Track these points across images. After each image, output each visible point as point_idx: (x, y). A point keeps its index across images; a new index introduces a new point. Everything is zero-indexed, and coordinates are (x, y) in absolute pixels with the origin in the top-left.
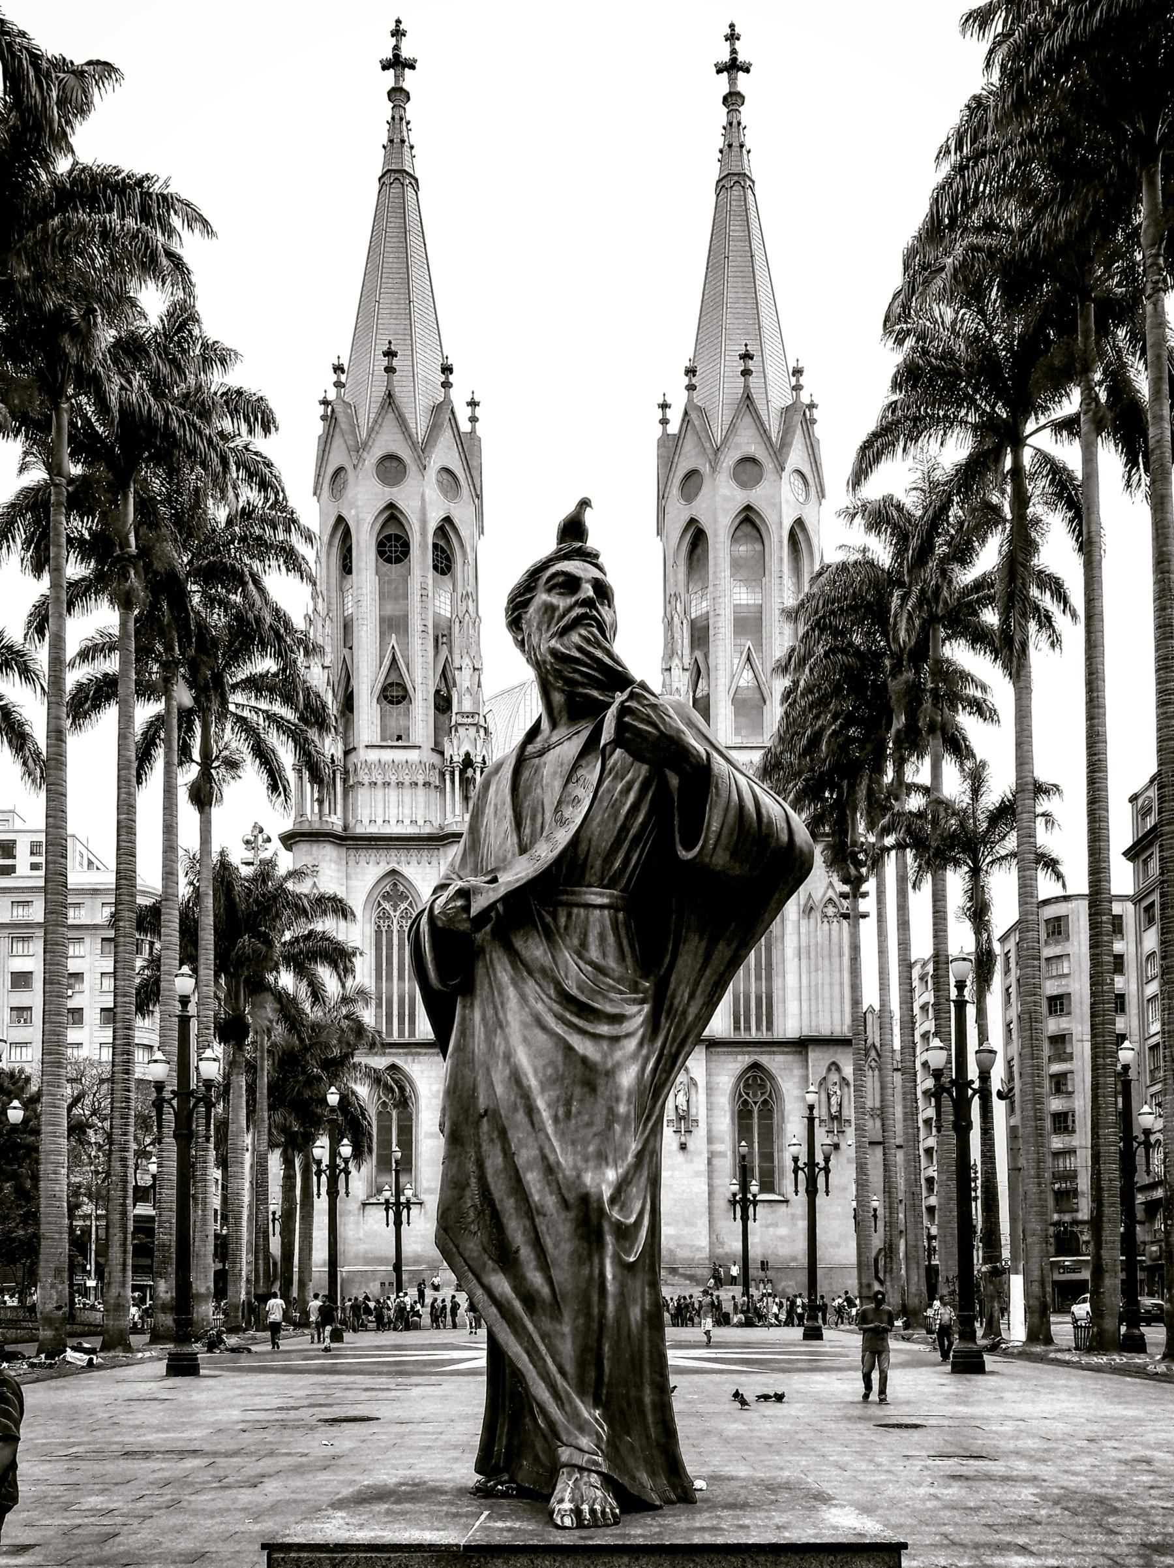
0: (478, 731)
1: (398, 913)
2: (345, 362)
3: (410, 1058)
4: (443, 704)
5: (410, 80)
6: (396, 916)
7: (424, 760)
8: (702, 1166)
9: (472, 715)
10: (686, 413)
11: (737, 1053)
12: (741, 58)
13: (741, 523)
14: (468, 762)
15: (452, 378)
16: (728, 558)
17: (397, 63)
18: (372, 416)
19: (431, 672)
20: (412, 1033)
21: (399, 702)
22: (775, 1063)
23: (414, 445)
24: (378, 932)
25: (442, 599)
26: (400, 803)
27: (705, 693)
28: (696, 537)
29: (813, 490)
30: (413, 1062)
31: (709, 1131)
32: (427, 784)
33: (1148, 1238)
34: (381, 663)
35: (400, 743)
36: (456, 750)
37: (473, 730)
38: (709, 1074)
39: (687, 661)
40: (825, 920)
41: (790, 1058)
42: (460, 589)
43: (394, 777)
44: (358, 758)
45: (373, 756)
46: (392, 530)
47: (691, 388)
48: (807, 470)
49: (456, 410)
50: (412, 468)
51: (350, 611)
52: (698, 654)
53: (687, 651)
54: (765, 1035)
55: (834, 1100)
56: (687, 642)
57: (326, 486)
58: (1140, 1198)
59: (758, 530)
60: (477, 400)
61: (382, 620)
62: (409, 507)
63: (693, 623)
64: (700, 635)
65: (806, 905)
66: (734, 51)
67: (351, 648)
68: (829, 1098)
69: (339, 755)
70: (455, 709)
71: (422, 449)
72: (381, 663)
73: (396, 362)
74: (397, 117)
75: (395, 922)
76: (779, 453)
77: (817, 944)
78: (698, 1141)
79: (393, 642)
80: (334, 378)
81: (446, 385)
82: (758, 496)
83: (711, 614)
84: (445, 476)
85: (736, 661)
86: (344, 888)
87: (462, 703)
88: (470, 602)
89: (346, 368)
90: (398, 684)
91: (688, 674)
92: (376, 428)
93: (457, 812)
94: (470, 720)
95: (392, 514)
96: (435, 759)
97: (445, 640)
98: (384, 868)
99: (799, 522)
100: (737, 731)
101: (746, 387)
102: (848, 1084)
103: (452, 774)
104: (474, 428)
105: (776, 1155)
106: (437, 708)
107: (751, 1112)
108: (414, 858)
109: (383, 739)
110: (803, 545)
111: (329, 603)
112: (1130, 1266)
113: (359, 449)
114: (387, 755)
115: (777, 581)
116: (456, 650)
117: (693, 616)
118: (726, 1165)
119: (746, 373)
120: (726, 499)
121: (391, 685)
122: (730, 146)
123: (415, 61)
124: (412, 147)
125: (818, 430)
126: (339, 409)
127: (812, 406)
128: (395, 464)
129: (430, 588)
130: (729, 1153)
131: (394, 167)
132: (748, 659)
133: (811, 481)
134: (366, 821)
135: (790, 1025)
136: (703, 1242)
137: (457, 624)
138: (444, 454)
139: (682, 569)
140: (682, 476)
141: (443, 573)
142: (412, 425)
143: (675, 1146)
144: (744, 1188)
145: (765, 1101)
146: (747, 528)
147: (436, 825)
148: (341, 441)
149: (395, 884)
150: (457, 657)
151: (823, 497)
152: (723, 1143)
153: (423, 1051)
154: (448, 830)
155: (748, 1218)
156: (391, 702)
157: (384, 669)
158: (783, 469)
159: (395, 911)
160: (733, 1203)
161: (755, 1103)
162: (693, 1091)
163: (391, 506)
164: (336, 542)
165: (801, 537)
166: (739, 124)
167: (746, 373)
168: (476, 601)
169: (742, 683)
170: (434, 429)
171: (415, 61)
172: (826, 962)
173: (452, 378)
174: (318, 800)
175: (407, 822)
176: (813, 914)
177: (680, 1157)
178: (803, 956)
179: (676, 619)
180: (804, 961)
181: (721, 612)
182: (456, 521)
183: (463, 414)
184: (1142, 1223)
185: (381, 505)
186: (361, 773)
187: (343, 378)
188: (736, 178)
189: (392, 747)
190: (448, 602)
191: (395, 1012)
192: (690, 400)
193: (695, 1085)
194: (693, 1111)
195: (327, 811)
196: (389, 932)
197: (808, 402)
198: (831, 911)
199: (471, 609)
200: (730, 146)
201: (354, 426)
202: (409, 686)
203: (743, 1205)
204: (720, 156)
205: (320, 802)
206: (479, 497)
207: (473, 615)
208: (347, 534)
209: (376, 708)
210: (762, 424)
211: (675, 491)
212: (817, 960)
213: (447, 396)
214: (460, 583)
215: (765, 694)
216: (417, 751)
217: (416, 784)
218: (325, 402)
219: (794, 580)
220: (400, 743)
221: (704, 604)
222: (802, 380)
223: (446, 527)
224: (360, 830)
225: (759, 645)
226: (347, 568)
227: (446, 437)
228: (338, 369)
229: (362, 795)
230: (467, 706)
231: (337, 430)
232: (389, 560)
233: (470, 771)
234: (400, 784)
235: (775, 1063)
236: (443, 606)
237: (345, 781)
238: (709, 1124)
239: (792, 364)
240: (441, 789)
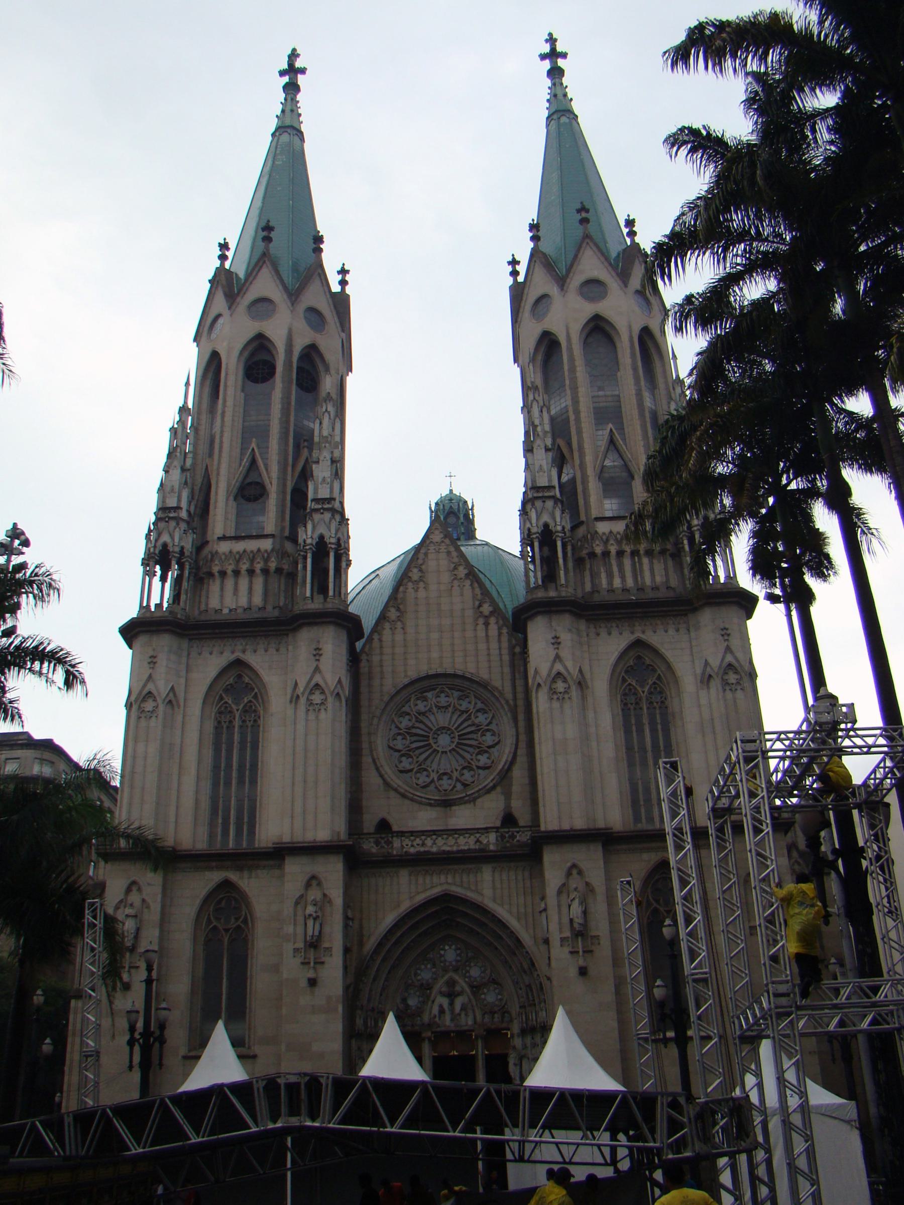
1: (241, 707)
4: (299, 496)
8: (608, 996)
12: (560, 48)
24: (218, 728)
27: (571, 476)
30: (250, 878)
32: (279, 571)
36: (308, 535)
39: (549, 442)
40: (727, 688)
45: (224, 547)
61: (244, 431)
65: (703, 673)
70: (311, 495)
78: (602, 964)
79: (254, 445)
86: (183, 681)
87: (316, 490)
90: (257, 483)
97: (306, 444)
98: (227, 657)
103: (305, 558)
110: (653, 350)
121: (250, 484)
122: (555, 96)
138: (312, 297)
143: (573, 972)
149: (240, 676)
156: (249, 500)
157: (242, 469)
159: (237, 704)
171: (306, 69)
176: (713, 683)
188: (562, 113)
196: (230, 727)
209: (232, 502)
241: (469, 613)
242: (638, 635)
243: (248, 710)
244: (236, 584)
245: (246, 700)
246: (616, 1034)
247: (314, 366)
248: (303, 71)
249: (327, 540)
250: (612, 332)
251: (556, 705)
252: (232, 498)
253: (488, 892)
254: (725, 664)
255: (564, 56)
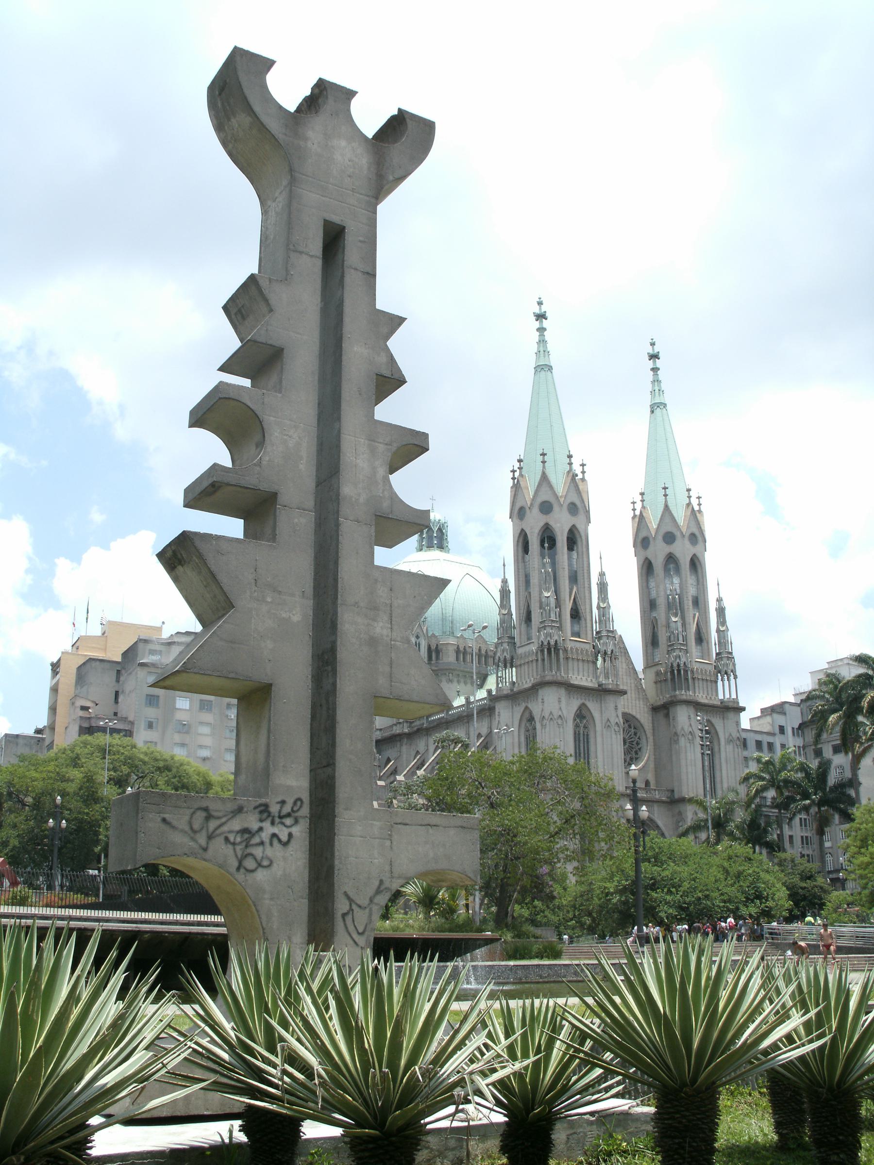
24: (575, 733)
98: (582, 702)
176: (731, 743)
196: (579, 734)
216: (588, 645)
234: (583, 661)
241: (633, 685)
242: (709, 718)
243: (585, 727)
244: (578, 665)
247: (575, 538)
250: (697, 564)
251: (688, 745)
253: (656, 815)
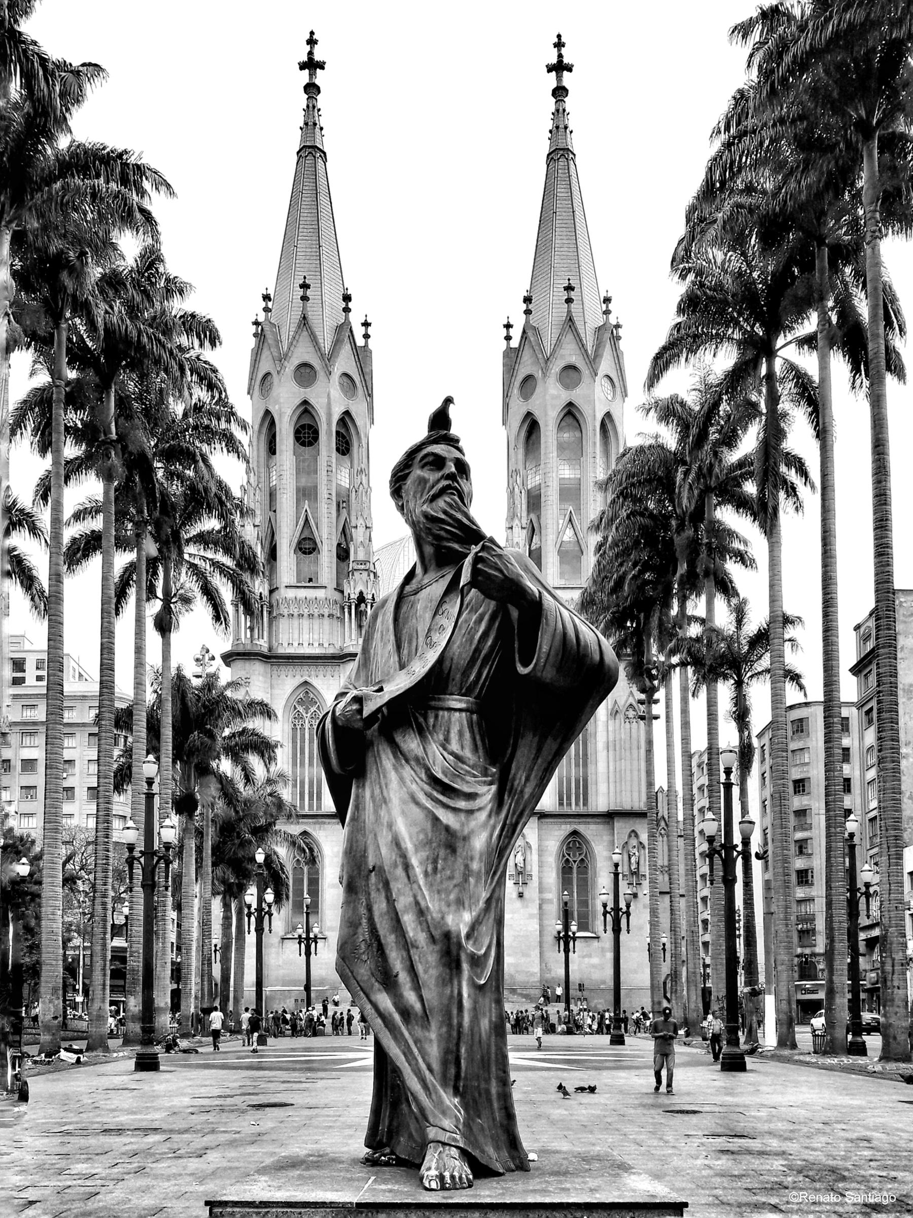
0: (369, 575)
1: (309, 715)
2: (271, 292)
3: (317, 826)
4: (343, 554)
5: (321, 78)
6: (307, 717)
7: (329, 597)
8: (536, 911)
9: (365, 562)
10: (524, 332)
11: (561, 823)
13: (565, 416)
14: (361, 599)
15: (350, 305)
16: (555, 443)
17: (311, 65)
18: (292, 333)
19: (334, 530)
20: (319, 807)
21: (310, 553)
22: (589, 830)
23: (322, 356)
24: (294, 729)
25: (343, 474)
26: (311, 630)
27: (538, 546)
28: (532, 426)
29: (618, 390)
31: (540, 883)
32: (331, 616)
33: (868, 967)
34: (297, 523)
35: (311, 584)
36: (352, 590)
37: (365, 574)
38: (540, 839)
39: (525, 521)
41: (601, 827)
42: (356, 466)
43: (306, 610)
44: (279, 595)
45: (291, 594)
46: (306, 421)
47: (528, 312)
48: (614, 376)
49: (354, 329)
50: (321, 374)
51: (274, 483)
52: (533, 516)
53: (524, 514)
54: (581, 809)
55: (633, 860)
56: (524, 507)
57: (257, 387)
58: (862, 936)
59: (578, 421)
60: (369, 321)
61: (298, 490)
62: (318, 404)
63: (529, 492)
64: (534, 501)
66: (560, 56)
67: (275, 511)
68: (630, 858)
69: (266, 593)
70: (352, 558)
71: (329, 359)
72: (297, 523)
73: (309, 293)
74: (311, 105)
75: (307, 722)
76: (593, 361)
77: (621, 739)
78: (531, 892)
79: (306, 507)
80: (263, 304)
81: (347, 310)
82: (577, 395)
83: (543, 485)
84: (345, 379)
85: (561, 522)
87: (357, 553)
88: (363, 476)
89: (272, 297)
90: (309, 539)
91: (525, 531)
92: (294, 343)
93: (353, 637)
94: (363, 567)
95: (306, 408)
96: (337, 596)
97: (344, 505)
98: (299, 680)
99: (608, 415)
100: (562, 575)
101: (569, 312)
102: (644, 847)
103: (350, 608)
104: (366, 343)
105: (590, 902)
106: (338, 557)
107: (571, 868)
108: (321, 672)
109: (298, 582)
110: (611, 433)
111: (259, 477)
112: (855, 990)
113: (282, 359)
114: (302, 593)
115: (592, 460)
116: (353, 513)
117: (529, 487)
118: (553, 909)
119: (569, 301)
120: (554, 397)
121: (304, 539)
122: (557, 127)
123: (324, 63)
124: (321, 129)
125: (622, 344)
126: (267, 328)
127: (618, 326)
128: (308, 370)
129: (334, 465)
130: (555, 900)
131: (308, 144)
132: (570, 520)
133: (617, 384)
134: (285, 645)
135: (600, 802)
136: (536, 969)
137: (354, 493)
138: (345, 363)
139: (521, 451)
140: (521, 380)
141: (344, 454)
142: (321, 341)
143: (515, 895)
144: (566, 927)
145: (582, 859)
146: (569, 420)
147: (338, 647)
148: (269, 353)
150: (353, 518)
151: (626, 396)
152: (550, 892)
153: (327, 821)
154: (346, 651)
155: (569, 951)
156: (304, 553)
157: (300, 527)
158: (596, 375)
160: (558, 939)
161: (575, 862)
162: (528, 853)
163: (305, 402)
164: (264, 430)
165: (609, 426)
166: (564, 110)
167: (569, 301)
168: (368, 475)
169: (566, 538)
170: (337, 343)
171: (324, 63)
172: (628, 753)
173: (350, 305)
174: (250, 627)
175: (316, 644)
177: (518, 904)
178: (611, 748)
179: (516, 489)
180: (611, 752)
181: (550, 484)
182: (353, 414)
183: (359, 331)
184: (864, 955)
185: (298, 401)
186: (282, 607)
187: (270, 304)
188: (561, 152)
189: (305, 587)
190: (347, 476)
191: (307, 791)
192: (527, 322)
193: (530, 847)
194: (528, 868)
195: (256, 636)
196: (303, 729)
197: (615, 323)
198: (631, 713)
199: (364, 482)
200: (557, 127)
201: (278, 342)
202: (318, 540)
203: (565, 940)
204: (550, 135)
205: (252, 629)
206: (370, 395)
207: (366, 486)
208: (272, 423)
209: (293, 557)
210: (581, 340)
211: (516, 391)
212: (621, 753)
213: (347, 318)
214: (356, 461)
215: (583, 547)
216: (323, 590)
217: (323, 616)
218: (256, 323)
219: (605, 459)
220: (311, 584)
221: (538, 478)
222: (611, 307)
223: (346, 419)
224: (280, 651)
225: (578, 509)
226: (272, 450)
227: (346, 350)
228: (266, 298)
229: (283, 625)
230: (361, 556)
231: (266, 344)
232: (303, 444)
233: (363, 605)
234: (311, 616)
235: (589, 830)
236: (343, 479)
237: (270, 613)
238: (540, 878)
239: (603, 295)
240: (341, 620)
245: (312, 710)
246: (538, 932)
248: (321, 66)
249: (365, 595)
252: (292, 551)
254: (628, 704)
255: (569, 69)
